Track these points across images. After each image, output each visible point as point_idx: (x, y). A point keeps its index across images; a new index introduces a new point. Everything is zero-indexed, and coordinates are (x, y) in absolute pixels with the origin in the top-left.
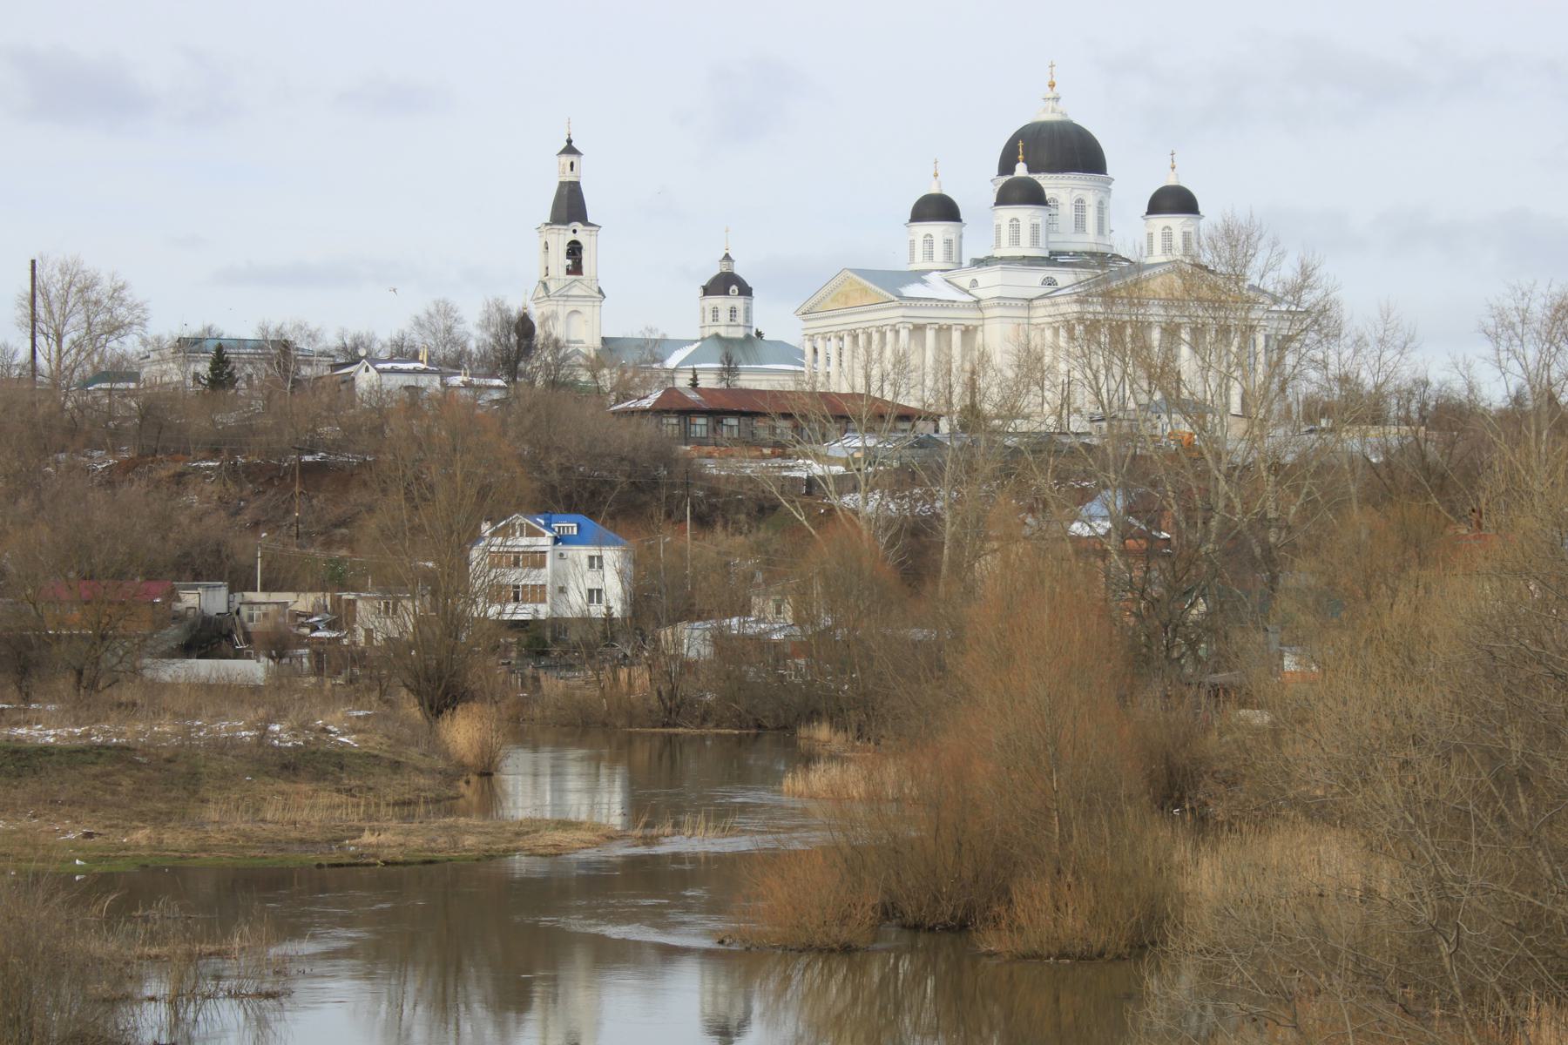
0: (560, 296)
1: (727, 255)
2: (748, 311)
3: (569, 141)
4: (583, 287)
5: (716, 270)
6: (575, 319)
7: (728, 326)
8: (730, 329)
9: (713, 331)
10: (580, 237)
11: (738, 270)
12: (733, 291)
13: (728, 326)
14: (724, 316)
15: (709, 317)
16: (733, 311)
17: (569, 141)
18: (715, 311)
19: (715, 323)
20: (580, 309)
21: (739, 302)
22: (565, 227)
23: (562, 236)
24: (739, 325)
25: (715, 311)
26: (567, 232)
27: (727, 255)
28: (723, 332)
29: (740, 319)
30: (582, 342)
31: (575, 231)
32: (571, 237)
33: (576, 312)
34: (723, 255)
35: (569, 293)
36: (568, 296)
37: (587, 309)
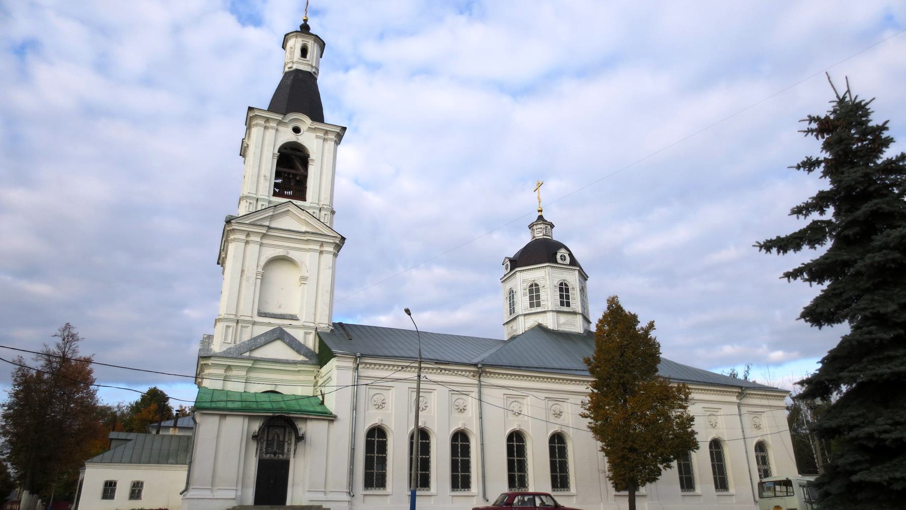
0: (252, 224)
1: (541, 218)
4: (303, 216)
6: (283, 276)
7: (558, 312)
8: (563, 319)
9: (531, 322)
10: (309, 140)
12: (563, 258)
13: (558, 312)
14: (549, 298)
15: (522, 302)
16: (564, 289)
18: (534, 291)
19: (539, 309)
20: (293, 254)
21: (572, 278)
22: (279, 117)
23: (271, 133)
25: (534, 291)
26: (281, 128)
27: (541, 218)
28: (550, 321)
29: (576, 304)
30: (293, 318)
31: (297, 130)
32: (287, 136)
35: (273, 225)
36: (269, 228)
37: (307, 258)
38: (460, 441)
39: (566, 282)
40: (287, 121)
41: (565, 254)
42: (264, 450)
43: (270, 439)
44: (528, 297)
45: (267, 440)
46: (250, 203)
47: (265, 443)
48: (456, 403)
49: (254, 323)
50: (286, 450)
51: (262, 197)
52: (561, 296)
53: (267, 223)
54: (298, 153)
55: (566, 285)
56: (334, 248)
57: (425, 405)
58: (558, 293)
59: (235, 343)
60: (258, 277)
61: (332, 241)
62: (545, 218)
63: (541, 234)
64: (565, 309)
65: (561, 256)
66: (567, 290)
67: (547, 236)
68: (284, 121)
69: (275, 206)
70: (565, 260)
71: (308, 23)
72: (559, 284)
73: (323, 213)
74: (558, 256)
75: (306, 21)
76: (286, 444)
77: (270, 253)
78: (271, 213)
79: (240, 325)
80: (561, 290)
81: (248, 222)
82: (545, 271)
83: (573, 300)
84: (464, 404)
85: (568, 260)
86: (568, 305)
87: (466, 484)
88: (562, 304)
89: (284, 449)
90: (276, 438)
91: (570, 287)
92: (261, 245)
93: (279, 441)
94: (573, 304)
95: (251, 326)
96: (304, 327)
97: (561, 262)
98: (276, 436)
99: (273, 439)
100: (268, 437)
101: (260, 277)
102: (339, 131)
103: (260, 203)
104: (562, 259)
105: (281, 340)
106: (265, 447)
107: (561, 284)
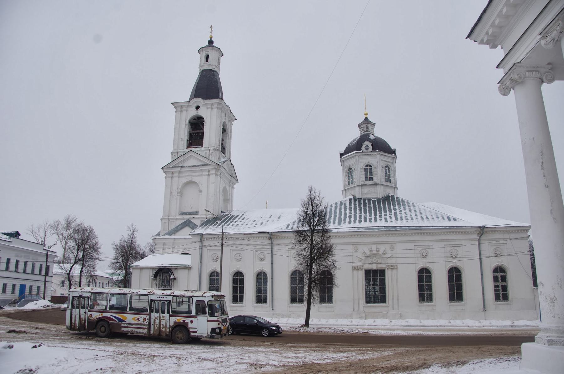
0: (173, 167)
1: (366, 119)
2: (388, 171)
3: (211, 42)
5: (356, 134)
6: (190, 192)
11: (378, 132)
12: (367, 148)
13: (362, 185)
14: (359, 176)
17: (211, 42)
20: (195, 179)
24: (376, 184)
27: (366, 119)
30: (197, 213)
33: (191, 183)
34: (363, 120)
35: (185, 165)
36: (181, 167)
38: (261, 278)
39: (370, 164)
40: (191, 105)
41: (368, 145)
42: (161, 284)
43: (163, 279)
44: (347, 178)
45: (162, 280)
46: (174, 155)
47: (161, 281)
48: (259, 256)
49: (177, 219)
50: (170, 284)
51: (180, 151)
52: (366, 174)
53: (181, 165)
54: (199, 120)
55: (370, 166)
56: (216, 171)
57: (241, 258)
58: (363, 173)
59: (168, 229)
60: (178, 194)
61: (213, 168)
62: (370, 119)
63: (363, 132)
64: (369, 183)
65: (366, 146)
66: (371, 169)
67: (367, 132)
68: (189, 105)
69: (183, 155)
70: (368, 149)
71: (213, 39)
72: (364, 166)
73: (211, 151)
74: (363, 148)
75: (211, 38)
76: (170, 281)
77: (184, 180)
78: (182, 159)
79: (170, 221)
80: (366, 170)
81: (171, 166)
82: (355, 159)
83: (375, 176)
84: (264, 256)
85: (371, 148)
86: (371, 179)
87: (265, 301)
88: (366, 180)
89: (170, 282)
90: (166, 278)
91: (373, 167)
92: (179, 177)
93: (167, 280)
94: (375, 179)
95: (175, 220)
96: (199, 218)
97: (366, 151)
98: (166, 277)
99: (165, 278)
100: (162, 279)
101: (179, 194)
102: (218, 102)
103: (179, 154)
104: (366, 149)
105: (188, 226)
106: (161, 282)
107: (367, 166)
